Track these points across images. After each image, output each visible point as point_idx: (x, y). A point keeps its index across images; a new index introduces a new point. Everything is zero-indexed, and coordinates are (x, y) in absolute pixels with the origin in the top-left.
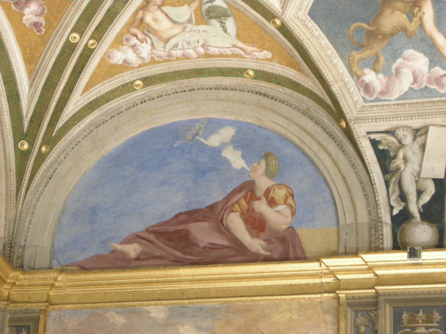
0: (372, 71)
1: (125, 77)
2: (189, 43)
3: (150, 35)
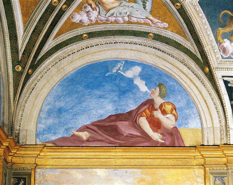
0: (228, 40)
1: (79, 31)
2: (120, 14)
3: (99, 6)
